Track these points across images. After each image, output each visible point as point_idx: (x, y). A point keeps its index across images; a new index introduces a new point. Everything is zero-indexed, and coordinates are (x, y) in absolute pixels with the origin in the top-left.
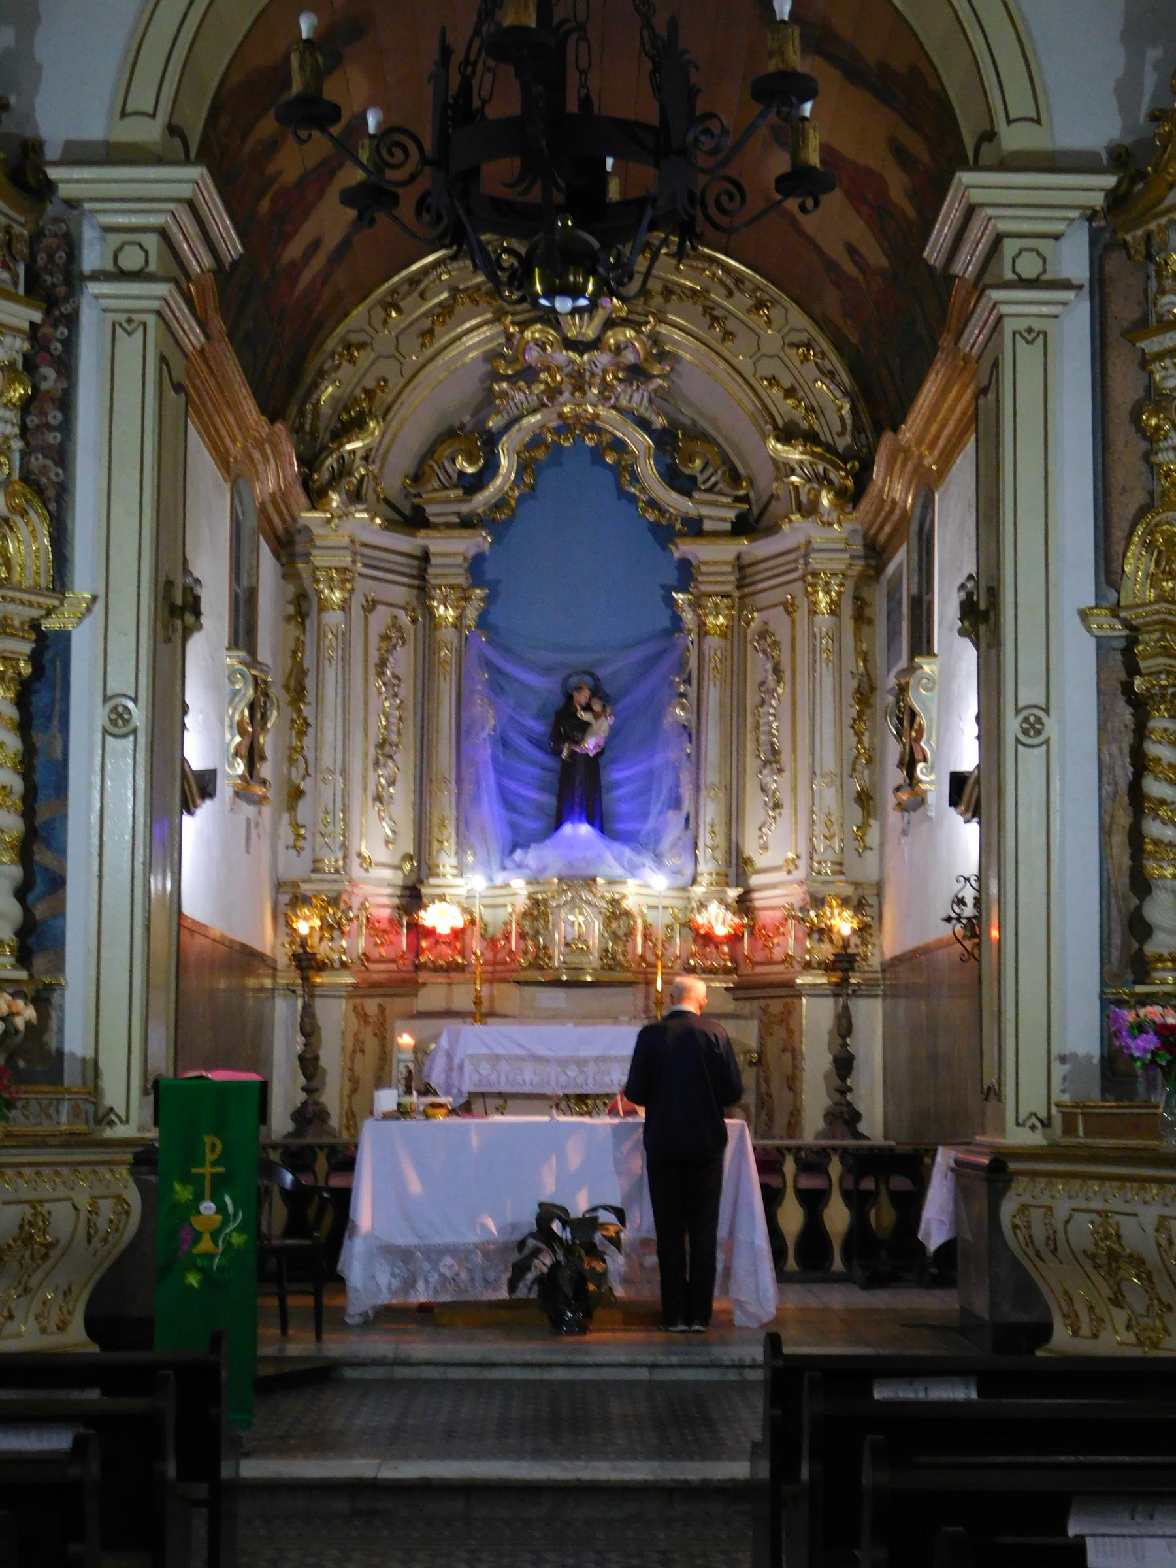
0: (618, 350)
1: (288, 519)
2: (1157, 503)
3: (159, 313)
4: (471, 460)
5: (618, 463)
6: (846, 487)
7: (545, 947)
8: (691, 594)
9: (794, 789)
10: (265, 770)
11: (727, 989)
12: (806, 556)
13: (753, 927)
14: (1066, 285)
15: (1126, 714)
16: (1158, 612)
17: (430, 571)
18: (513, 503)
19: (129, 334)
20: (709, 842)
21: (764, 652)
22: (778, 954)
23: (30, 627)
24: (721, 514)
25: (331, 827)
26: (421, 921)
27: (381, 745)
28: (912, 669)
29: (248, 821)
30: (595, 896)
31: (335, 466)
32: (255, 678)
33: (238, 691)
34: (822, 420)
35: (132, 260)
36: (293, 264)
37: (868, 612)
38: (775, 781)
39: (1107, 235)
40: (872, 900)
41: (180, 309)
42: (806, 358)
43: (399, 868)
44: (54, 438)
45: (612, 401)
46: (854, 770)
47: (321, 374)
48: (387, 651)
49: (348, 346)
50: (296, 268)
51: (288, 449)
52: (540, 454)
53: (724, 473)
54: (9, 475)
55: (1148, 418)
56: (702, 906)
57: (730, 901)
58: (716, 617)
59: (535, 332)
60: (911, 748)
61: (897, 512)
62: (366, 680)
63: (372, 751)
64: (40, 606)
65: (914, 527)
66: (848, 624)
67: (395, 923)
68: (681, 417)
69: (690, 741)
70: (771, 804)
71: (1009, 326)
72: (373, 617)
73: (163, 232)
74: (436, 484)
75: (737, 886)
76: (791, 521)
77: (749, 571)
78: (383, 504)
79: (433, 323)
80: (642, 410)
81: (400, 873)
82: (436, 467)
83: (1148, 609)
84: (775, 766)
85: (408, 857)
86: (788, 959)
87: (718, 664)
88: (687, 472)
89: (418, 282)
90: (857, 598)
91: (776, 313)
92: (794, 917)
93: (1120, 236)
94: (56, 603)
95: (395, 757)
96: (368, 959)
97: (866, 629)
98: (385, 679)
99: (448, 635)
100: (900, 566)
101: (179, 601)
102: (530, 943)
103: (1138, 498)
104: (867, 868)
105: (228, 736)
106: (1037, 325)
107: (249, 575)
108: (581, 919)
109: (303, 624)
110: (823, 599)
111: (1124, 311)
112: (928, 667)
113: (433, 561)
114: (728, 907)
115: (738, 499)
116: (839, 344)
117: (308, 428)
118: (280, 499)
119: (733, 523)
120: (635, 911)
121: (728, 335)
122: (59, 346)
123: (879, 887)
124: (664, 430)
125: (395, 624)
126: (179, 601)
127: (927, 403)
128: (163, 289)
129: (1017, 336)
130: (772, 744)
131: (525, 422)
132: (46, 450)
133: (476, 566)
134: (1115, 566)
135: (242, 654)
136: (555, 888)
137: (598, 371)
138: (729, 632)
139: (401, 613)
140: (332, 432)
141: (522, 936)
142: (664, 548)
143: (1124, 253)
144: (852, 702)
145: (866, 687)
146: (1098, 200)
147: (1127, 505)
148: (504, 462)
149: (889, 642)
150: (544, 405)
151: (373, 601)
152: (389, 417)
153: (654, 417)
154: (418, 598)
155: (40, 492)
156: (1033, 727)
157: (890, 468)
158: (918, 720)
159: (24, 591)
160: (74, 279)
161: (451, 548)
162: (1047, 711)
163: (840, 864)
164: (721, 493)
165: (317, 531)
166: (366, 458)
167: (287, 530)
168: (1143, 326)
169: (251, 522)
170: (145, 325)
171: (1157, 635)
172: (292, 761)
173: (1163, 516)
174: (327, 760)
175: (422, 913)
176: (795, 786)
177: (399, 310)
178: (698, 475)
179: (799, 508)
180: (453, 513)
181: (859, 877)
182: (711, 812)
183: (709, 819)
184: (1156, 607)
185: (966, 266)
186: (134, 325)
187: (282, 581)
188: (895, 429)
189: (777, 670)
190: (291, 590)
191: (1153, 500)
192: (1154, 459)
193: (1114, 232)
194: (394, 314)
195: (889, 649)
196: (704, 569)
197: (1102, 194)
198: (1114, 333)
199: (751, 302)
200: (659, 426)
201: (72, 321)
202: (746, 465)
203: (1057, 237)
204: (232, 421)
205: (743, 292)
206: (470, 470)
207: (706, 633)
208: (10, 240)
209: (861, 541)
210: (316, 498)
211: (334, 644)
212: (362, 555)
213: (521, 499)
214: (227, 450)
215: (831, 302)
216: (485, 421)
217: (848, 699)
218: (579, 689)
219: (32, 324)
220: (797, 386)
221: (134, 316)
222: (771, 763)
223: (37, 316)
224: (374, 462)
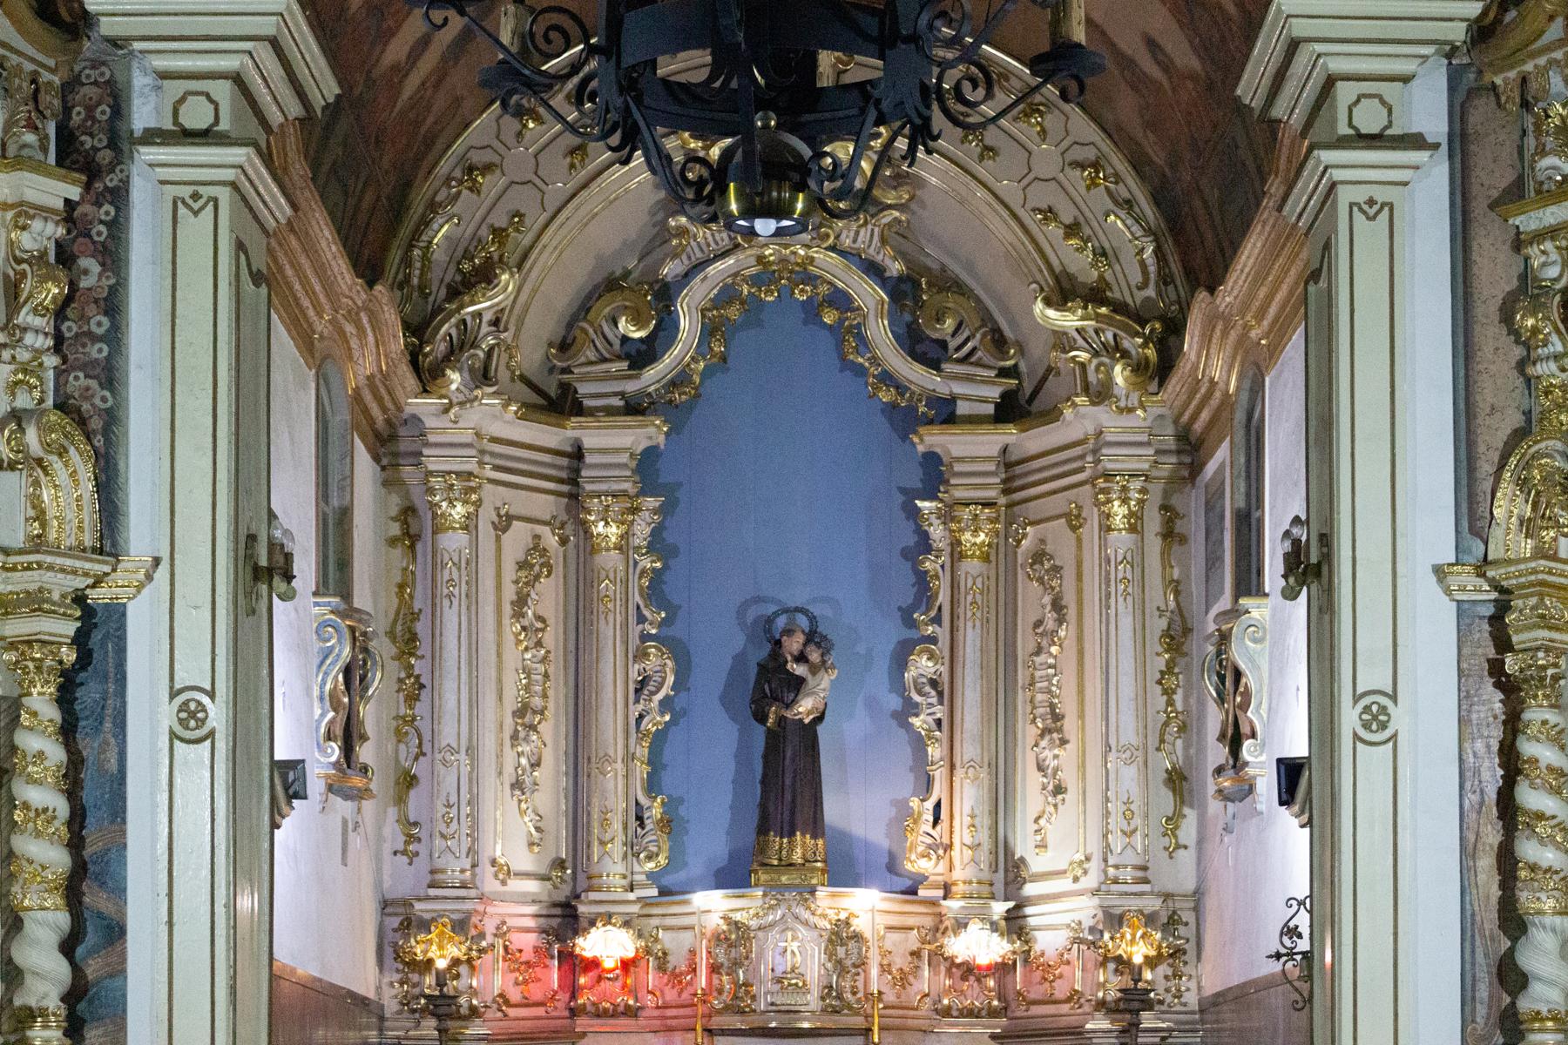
1: (390, 405)
2: (1536, 429)
3: (234, 185)
4: (638, 322)
5: (841, 321)
6: (1147, 358)
8: (941, 501)
9: (1082, 766)
10: (365, 753)
11: (993, 1037)
12: (1095, 452)
14: (1415, 141)
15: (1494, 700)
16: (1535, 571)
17: (583, 473)
18: (697, 379)
19: (196, 213)
21: (1041, 580)
22: (1061, 990)
23: (73, 600)
24: (982, 393)
25: (454, 826)
26: (577, 951)
27: (520, 713)
28: (1235, 613)
29: (345, 822)
31: (454, 332)
32: (352, 630)
33: (332, 647)
34: (1117, 267)
35: (197, 116)
36: (395, 68)
37: (1179, 526)
38: (1056, 757)
39: (1472, 76)
40: (1189, 916)
41: (266, 186)
42: (1093, 184)
43: (544, 878)
44: (99, 351)
45: (831, 241)
46: (1162, 741)
47: (433, 207)
48: (527, 584)
49: (470, 169)
50: (400, 71)
51: (391, 317)
53: (984, 335)
54: (41, 401)
55: (1522, 318)
56: (961, 925)
57: (995, 918)
58: (975, 532)
60: (1236, 718)
61: (1218, 394)
62: (499, 623)
63: (509, 721)
64: (86, 575)
65: (1240, 416)
66: (1154, 544)
67: (542, 953)
68: (929, 263)
69: (941, 703)
70: (1051, 787)
71: (1345, 196)
72: (505, 537)
73: (237, 79)
74: (591, 355)
75: (1006, 899)
76: (1074, 405)
77: (1018, 470)
78: (521, 387)
80: (871, 251)
81: (548, 884)
82: (591, 331)
83: (1522, 567)
84: (1055, 735)
85: (560, 864)
86: (1073, 997)
87: (978, 598)
88: (935, 336)
90: (1165, 507)
91: (1052, 121)
92: (1081, 941)
93: (1488, 77)
94: (107, 569)
95: (540, 728)
96: (507, 1003)
97: (1175, 547)
98: (526, 622)
99: (610, 560)
100: (1222, 466)
101: (263, 562)
102: (725, 978)
103: (1517, 420)
104: (1181, 874)
105: (318, 712)
106: (1381, 194)
107: (342, 489)
108: (794, 946)
109: (412, 547)
110: (1119, 511)
111: (1493, 177)
112: (1258, 610)
113: (589, 459)
114: (994, 927)
115: (1004, 373)
116: (1139, 164)
117: (415, 281)
118: (379, 384)
119: (997, 405)
120: (868, 934)
121: (988, 151)
122: (102, 228)
123: (1198, 896)
124: (901, 279)
125: (537, 547)
126: (263, 562)
127: (1252, 261)
128: (238, 154)
129: (1355, 209)
130: (1052, 706)
131: (711, 270)
132: (88, 367)
134: (1483, 509)
135: (335, 600)
136: (760, 903)
138: (993, 552)
139: (545, 531)
140: (449, 286)
141: (714, 969)
142: (904, 437)
143: (1493, 98)
144: (1160, 650)
145: (1177, 627)
146: (1458, 33)
147: (1495, 432)
148: (684, 323)
149: (1208, 570)
150: (737, 246)
151: (507, 514)
152: (528, 265)
153: (888, 262)
154: (568, 510)
155: (82, 422)
156: (1376, 719)
157: (1206, 340)
158: (1244, 680)
159: (64, 555)
160: (120, 142)
161: (613, 442)
162: (1394, 698)
163: (1145, 868)
164: (978, 364)
165: (430, 422)
166: (495, 323)
167: (388, 422)
168: (1516, 194)
169: (341, 416)
170: (216, 200)
171: (1533, 601)
172: (400, 736)
173: (1543, 445)
174: (449, 732)
175: (580, 941)
176: (1084, 762)
178: (948, 338)
179: (1086, 389)
180: (615, 394)
181: (1170, 888)
182: (969, 798)
183: (967, 810)
184: (1533, 565)
185: (1290, 109)
186: (201, 202)
187: (383, 491)
188: (1212, 290)
189: (1057, 606)
190: (395, 503)
191: (1529, 421)
192: (1530, 371)
193: (1480, 72)
194: (531, 125)
195: (1207, 576)
197: (1465, 24)
198: (1479, 207)
200: (895, 274)
201: (119, 196)
202: (1013, 323)
203: (1406, 79)
204: (318, 288)
207: (962, 556)
208: (37, 91)
209: (1170, 430)
210: (428, 376)
211: (455, 576)
212: (492, 454)
213: (705, 375)
214: (310, 325)
215: (1126, 107)
216: (661, 262)
217: (1154, 645)
218: (789, 632)
219: (67, 201)
220: (1081, 219)
221: (201, 190)
222: (1050, 731)
223: (75, 193)
224: (506, 330)
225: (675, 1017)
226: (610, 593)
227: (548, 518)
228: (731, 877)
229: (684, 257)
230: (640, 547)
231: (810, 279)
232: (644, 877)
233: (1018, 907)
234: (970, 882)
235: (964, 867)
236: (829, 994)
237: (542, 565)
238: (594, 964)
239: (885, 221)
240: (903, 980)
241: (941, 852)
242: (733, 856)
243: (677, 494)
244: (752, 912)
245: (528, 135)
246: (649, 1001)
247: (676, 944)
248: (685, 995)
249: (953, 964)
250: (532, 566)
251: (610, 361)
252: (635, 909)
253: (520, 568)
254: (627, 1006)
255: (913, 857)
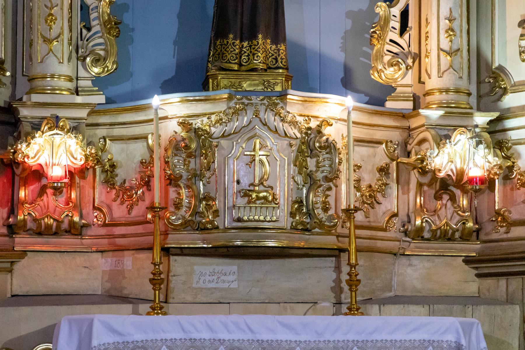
7: (207, 198)
13: (510, 169)
20: (445, 44)
26: (20, 158)
30: (283, 120)
120: (340, 145)
136: (222, 107)
183: (444, 12)
225: (124, 236)
228: (191, 78)
232: (89, 83)
233: (499, 119)
234: (447, 91)
235: (439, 74)
236: (299, 209)
238: (38, 174)
240: (371, 198)
241: (410, 61)
242: (179, 67)
244: (214, 118)
246: (95, 218)
247: (127, 157)
248: (135, 212)
249: (434, 178)
252: (83, 113)
254: (72, 223)
255: (380, 67)
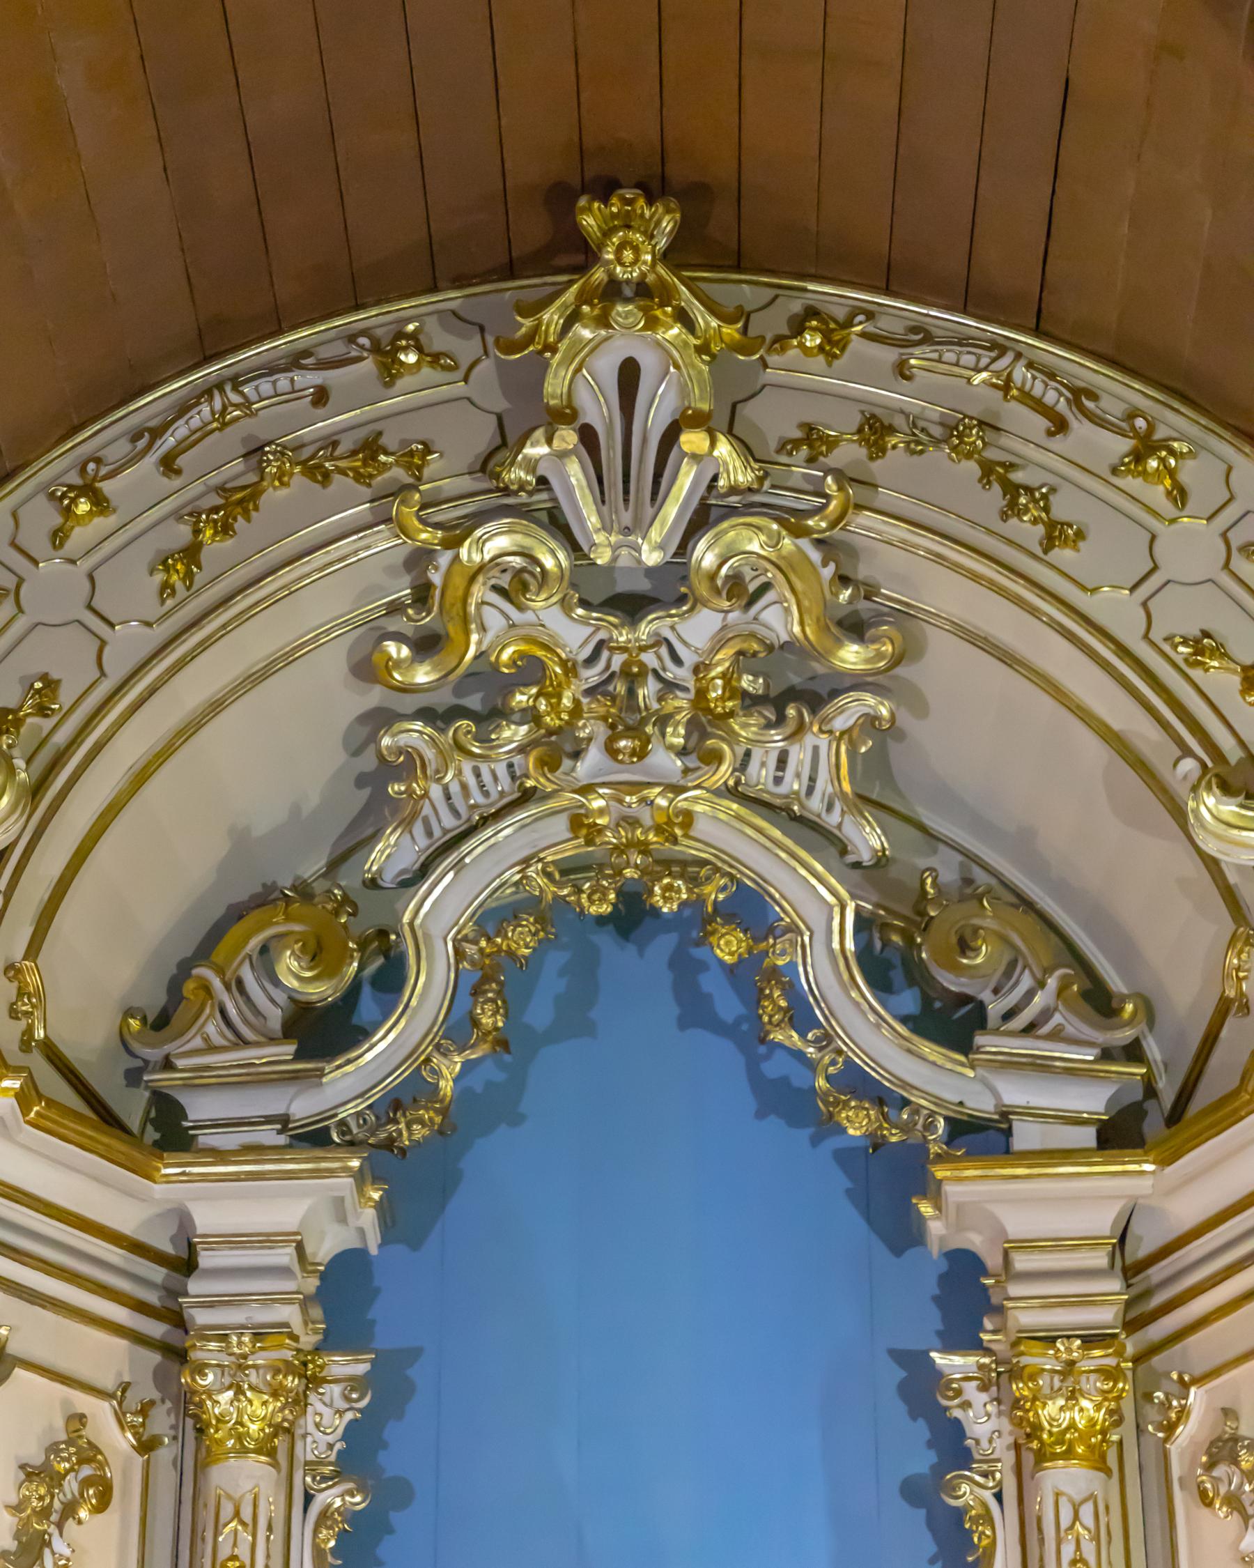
0: (741, 591)
24: (1063, 1095)
48: (44, 1513)
52: (521, 939)
59: (497, 542)
77: (1157, 1273)
79: (197, 532)
80: (815, 804)
82: (217, 983)
89: (157, 433)
99: (245, 1478)
113: (206, 1259)
121: (1055, 533)
124: (881, 861)
131: (474, 847)
133: (343, 1293)
137: (682, 674)
154: (161, 1378)
164: (1056, 1036)
177: (101, 504)
178: (986, 996)
180: (268, 1120)
194: (83, 507)
196: (1021, 1262)
199: (1122, 445)
202: (1127, 955)
205: (1098, 421)
206: (321, 991)
226: (243, 1552)
227: (109, 1384)
229: (418, 828)
230: (321, 1463)
231: (690, 870)
237: (86, 1483)
239: (840, 724)
243: (410, 1372)
245: (80, 536)
250: (56, 1480)
251: (257, 1044)
253: (30, 1476)
